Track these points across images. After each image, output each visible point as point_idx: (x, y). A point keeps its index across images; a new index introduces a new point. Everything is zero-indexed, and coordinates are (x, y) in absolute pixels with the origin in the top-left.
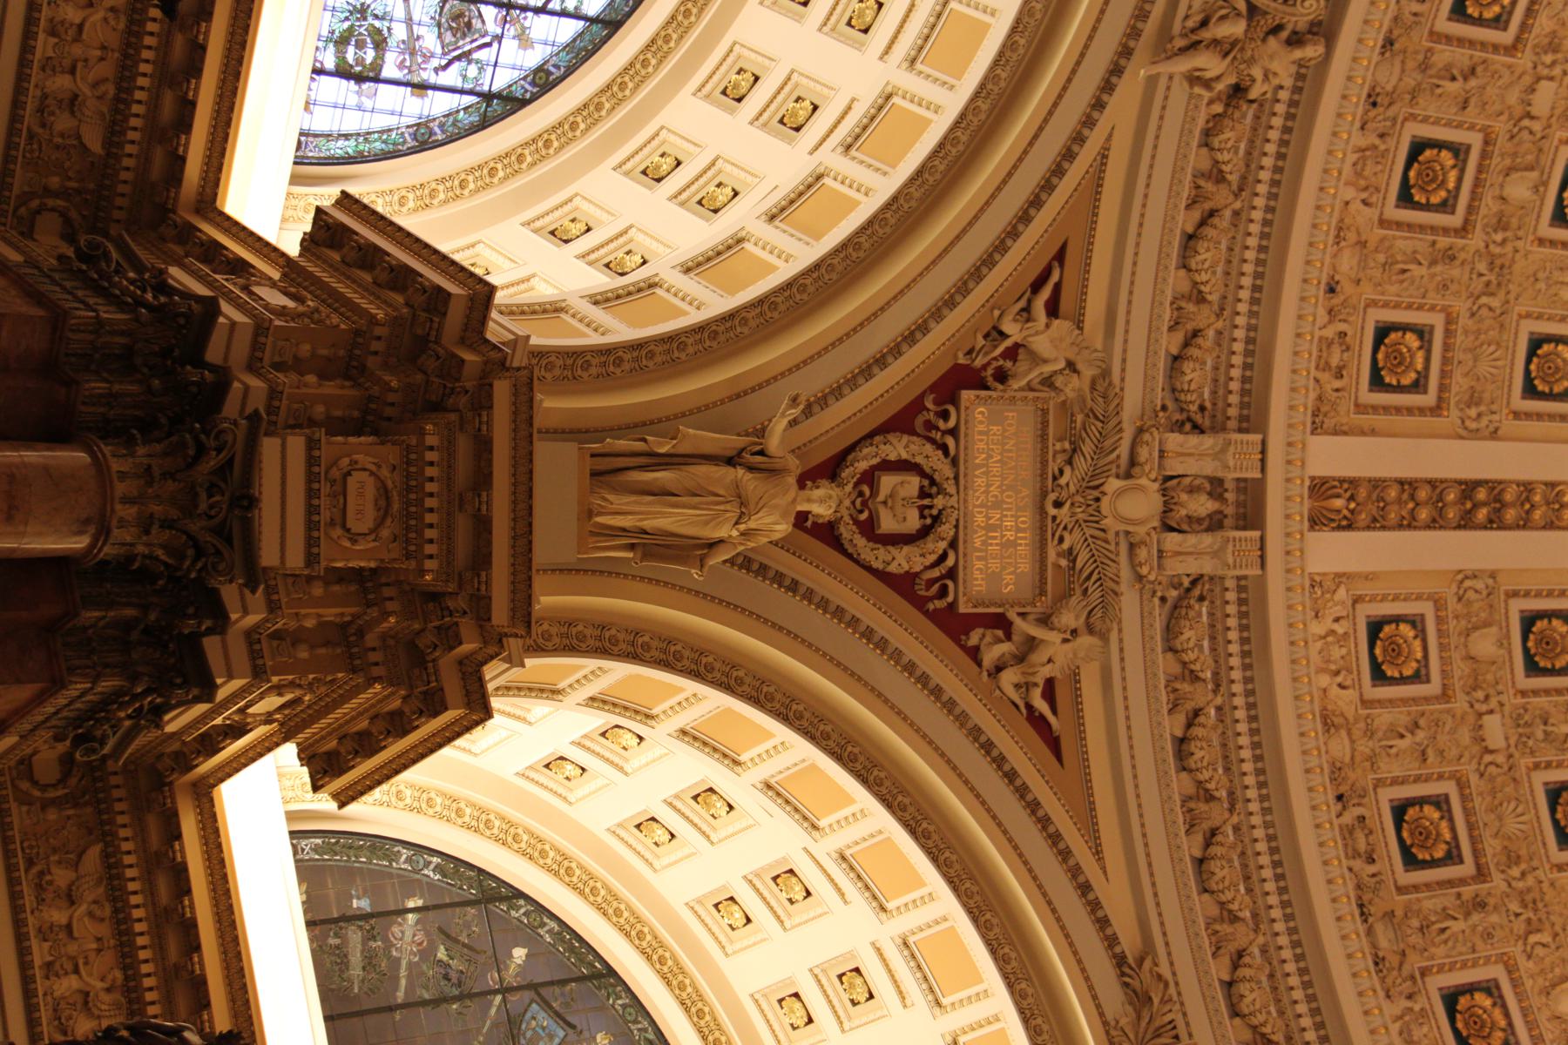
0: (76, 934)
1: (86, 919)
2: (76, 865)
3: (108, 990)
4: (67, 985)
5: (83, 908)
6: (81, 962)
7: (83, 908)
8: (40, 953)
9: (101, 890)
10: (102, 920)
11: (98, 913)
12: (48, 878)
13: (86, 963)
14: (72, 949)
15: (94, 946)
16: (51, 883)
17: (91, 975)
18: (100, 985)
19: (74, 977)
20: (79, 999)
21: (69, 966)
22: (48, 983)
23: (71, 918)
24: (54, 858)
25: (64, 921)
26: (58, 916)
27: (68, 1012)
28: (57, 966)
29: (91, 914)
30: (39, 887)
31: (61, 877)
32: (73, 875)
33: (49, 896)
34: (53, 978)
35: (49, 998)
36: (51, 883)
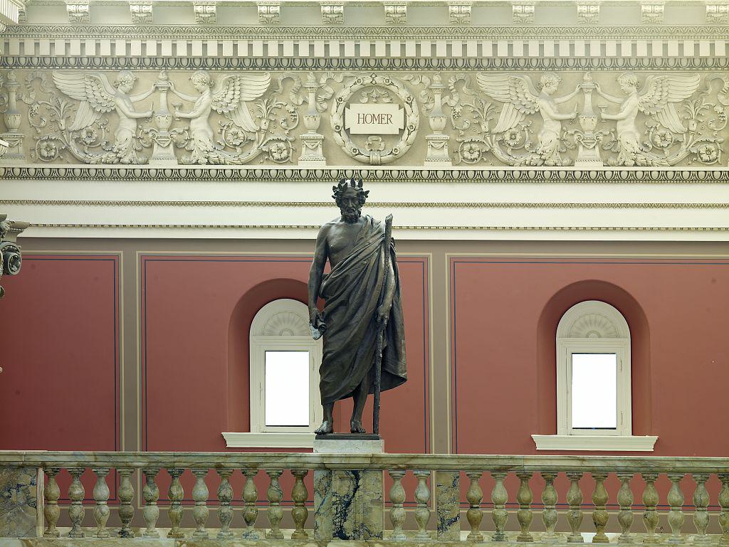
0: (148, 114)
1: (133, 99)
3: (212, 86)
4: (629, 136)
5: (120, 102)
6: (178, 114)
7: (120, 102)
8: (589, 161)
9: (103, 77)
10: (136, 81)
11: (128, 87)
12: (507, 137)
13: (181, 107)
14: (163, 122)
15: (163, 96)
16: (513, 136)
18: (206, 97)
19: (193, 124)
20: (217, 120)
21: (180, 128)
22: (197, 155)
23: (130, 118)
24: (485, 127)
25: (133, 125)
26: (126, 132)
27: (230, 137)
28: (181, 139)
29: (128, 93)
30: (519, 149)
31: (507, 121)
32: (83, 104)
33: (104, 136)
34: (191, 146)
35: (641, 158)
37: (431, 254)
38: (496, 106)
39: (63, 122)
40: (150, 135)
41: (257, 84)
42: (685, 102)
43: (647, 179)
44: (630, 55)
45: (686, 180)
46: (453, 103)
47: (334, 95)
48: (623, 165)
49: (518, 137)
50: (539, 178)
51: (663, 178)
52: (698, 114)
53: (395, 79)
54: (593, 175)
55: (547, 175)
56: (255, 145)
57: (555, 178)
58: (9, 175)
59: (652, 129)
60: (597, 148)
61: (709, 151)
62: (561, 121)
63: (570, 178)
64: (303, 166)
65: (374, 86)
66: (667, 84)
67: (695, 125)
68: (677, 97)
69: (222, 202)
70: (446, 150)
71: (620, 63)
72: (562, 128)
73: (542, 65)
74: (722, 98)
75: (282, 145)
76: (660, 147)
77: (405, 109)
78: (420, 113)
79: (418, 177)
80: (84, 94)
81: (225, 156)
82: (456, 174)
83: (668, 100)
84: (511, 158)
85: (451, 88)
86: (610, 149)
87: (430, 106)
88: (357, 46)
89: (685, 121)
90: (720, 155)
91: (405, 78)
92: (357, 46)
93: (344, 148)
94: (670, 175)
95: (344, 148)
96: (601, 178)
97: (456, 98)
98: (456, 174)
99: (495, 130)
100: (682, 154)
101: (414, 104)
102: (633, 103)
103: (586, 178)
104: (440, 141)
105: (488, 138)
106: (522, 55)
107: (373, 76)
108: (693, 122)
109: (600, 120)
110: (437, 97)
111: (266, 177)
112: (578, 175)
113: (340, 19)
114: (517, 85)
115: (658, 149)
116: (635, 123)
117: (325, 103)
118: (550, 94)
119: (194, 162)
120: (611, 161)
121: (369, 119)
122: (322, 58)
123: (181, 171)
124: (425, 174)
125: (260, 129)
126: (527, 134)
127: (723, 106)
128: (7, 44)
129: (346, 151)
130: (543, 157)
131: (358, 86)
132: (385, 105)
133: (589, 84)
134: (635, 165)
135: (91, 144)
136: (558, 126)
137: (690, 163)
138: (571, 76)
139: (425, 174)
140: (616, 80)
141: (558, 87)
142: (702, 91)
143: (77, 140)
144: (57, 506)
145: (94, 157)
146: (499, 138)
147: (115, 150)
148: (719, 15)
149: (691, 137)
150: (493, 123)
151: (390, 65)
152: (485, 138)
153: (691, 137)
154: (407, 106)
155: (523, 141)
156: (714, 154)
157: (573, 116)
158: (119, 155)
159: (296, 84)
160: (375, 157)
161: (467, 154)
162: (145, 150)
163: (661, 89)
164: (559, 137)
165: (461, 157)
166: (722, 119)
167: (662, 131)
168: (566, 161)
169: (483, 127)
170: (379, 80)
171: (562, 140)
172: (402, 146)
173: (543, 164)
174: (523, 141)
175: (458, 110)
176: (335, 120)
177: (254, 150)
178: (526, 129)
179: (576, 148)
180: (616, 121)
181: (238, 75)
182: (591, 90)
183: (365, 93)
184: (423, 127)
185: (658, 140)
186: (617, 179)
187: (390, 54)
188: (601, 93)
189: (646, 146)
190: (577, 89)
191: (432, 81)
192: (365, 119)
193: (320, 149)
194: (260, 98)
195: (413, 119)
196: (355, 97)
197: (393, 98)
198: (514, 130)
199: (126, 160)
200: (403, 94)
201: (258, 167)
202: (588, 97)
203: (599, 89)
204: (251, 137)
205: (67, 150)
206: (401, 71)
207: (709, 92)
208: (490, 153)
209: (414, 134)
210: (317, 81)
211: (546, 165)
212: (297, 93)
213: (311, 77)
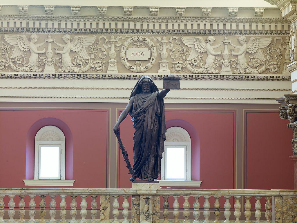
2: (12, 47)
4: (67, 59)
8: (49, 70)
12: (16, 59)
16: (19, 60)
17: (63, 48)
30: (21, 65)
36: (19, 60)
37: (110, 108)
38: (12, 47)
39: (7, 55)
40: (44, 60)
41: (89, 40)
42: (90, 47)
43: (73, 77)
44: (45, 27)
45: (250, 79)
46: (170, 48)
47: (122, 45)
48: (64, 72)
49: (21, 60)
50: (29, 77)
51: (79, 77)
52: (95, 52)
53: (147, 37)
54: (113, 76)
55: (32, 76)
56: (88, 65)
57: (35, 77)
58: (3, 77)
59: (76, 58)
60: (53, 65)
61: (99, 66)
62: (38, 54)
63: (41, 77)
64: (108, 73)
65: (138, 41)
66: (258, 41)
67: (94, 56)
68: (87, 44)
69: (39, 88)
70: (168, 67)
71: (41, 30)
72: (39, 57)
73: (205, 33)
74: (105, 46)
75: (100, 64)
76: (255, 66)
77: (151, 51)
78: (157, 51)
79: (104, 78)
80: (16, 44)
81: (76, 69)
82: (57, 76)
83: (83, 46)
84: (17, 68)
85: (170, 42)
86: (59, 64)
87: (160, 49)
88: (135, 25)
89: (90, 55)
90: (103, 69)
91: (151, 38)
92: (135, 25)
93: (125, 66)
94: (82, 76)
95: (125, 66)
96: (54, 77)
97: (172, 45)
98: (57, 76)
99: (11, 57)
100: (88, 67)
101: (155, 48)
102: (243, 49)
103: (48, 77)
104: (165, 63)
105: (8, 60)
106: (83, 28)
107: (139, 37)
108: (93, 55)
109: (55, 53)
110: (164, 46)
111: (91, 78)
112: (44, 76)
113: (79, 13)
114: (20, 39)
115: (78, 66)
116: (69, 54)
117: (118, 48)
118: (211, 45)
119: (63, 71)
120: (59, 70)
121: (135, 54)
122: (83, 29)
123: (37, 75)
124: (107, 76)
125: (91, 59)
126: (24, 59)
127: (105, 48)
128: (2, 23)
129: (127, 67)
130: (31, 68)
131: (131, 41)
132: (143, 48)
133: (227, 41)
134: (69, 72)
135: (19, 64)
136: (37, 55)
137: (91, 71)
138: (43, 35)
139: (107, 76)
140: (62, 38)
141: (38, 40)
142: (96, 43)
143: (13, 62)
144: (24, 210)
145: (21, 69)
146: (190, 62)
147: (29, 66)
148: (181, 13)
149: (92, 61)
150: (10, 54)
151: (148, 32)
152: (7, 60)
153: (92, 61)
154: (152, 49)
155: (22, 62)
156: (101, 68)
157: (43, 52)
158: (31, 68)
159: (107, 41)
160: (139, 69)
161: (177, 69)
162: (42, 66)
163: (80, 42)
164: (37, 60)
165: (174, 69)
166: (105, 54)
167: (80, 58)
168: (41, 70)
169: (6, 56)
170: (141, 39)
171: (39, 62)
172: (149, 65)
173: (31, 71)
174: (22, 62)
175: (173, 50)
176: (123, 54)
177: (88, 67)
178: (24, 57)
179: (45, 65)
180: (62, 54)
181: (82, 36)
182: (51, 42)
183: (135, 43)
184: (160, 57)
185: (78, 61)
186: (60, 77)
187: (35, 26)
188: (56, 43)
189: (74, 64)
190: (46, 41)
191: (162, 39)
192: (137, 54)
193: (116, 66)
194: (91, 46)
195: (155, 54)
196: (132, 44)
197: (147, 45)
198: (19, 57)
199: (34, 70)
200: (151, 44)
201: (88, 74)
202: (50, 45)
203: (55, 41)
204: (88, 62)
205: (9, 66)
206: (100, 34)
207: (100, 43)
208: (186, 68)
209: (154, 60)
210: (115, 39)
211: (32, 72)
212: (106, 44)
213: (113, 37)
